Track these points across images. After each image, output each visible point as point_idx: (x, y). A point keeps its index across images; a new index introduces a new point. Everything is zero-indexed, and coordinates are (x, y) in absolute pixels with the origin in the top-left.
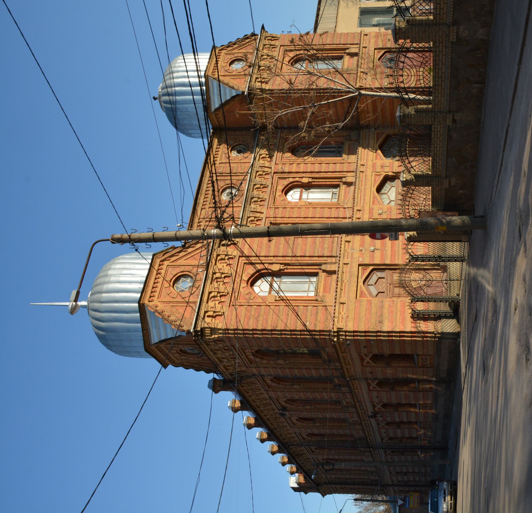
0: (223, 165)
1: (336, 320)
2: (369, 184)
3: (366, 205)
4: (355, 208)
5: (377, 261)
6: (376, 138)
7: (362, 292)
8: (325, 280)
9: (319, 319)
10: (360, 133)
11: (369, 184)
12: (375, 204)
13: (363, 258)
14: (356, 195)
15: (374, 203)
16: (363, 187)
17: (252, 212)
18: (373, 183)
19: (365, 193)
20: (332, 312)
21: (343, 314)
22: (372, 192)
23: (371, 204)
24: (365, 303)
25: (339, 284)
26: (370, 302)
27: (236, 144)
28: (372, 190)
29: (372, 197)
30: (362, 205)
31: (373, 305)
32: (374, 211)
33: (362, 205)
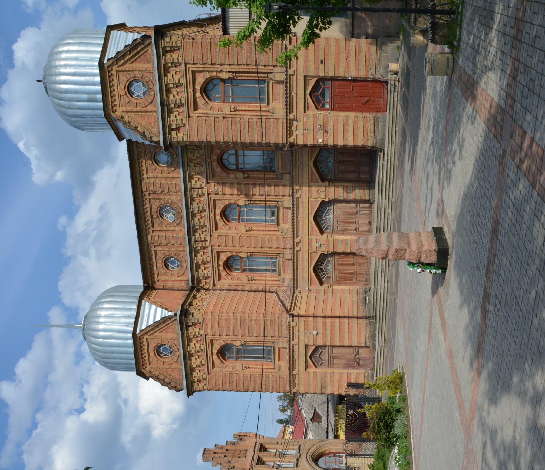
0: (152, 181)
3: (304, 237)
6: (310, 152)
8: (279, 351)
11: (306, 212)
13: (308, 340)
16: (300, 215)
20: (288, 380)
32: (313, 244)
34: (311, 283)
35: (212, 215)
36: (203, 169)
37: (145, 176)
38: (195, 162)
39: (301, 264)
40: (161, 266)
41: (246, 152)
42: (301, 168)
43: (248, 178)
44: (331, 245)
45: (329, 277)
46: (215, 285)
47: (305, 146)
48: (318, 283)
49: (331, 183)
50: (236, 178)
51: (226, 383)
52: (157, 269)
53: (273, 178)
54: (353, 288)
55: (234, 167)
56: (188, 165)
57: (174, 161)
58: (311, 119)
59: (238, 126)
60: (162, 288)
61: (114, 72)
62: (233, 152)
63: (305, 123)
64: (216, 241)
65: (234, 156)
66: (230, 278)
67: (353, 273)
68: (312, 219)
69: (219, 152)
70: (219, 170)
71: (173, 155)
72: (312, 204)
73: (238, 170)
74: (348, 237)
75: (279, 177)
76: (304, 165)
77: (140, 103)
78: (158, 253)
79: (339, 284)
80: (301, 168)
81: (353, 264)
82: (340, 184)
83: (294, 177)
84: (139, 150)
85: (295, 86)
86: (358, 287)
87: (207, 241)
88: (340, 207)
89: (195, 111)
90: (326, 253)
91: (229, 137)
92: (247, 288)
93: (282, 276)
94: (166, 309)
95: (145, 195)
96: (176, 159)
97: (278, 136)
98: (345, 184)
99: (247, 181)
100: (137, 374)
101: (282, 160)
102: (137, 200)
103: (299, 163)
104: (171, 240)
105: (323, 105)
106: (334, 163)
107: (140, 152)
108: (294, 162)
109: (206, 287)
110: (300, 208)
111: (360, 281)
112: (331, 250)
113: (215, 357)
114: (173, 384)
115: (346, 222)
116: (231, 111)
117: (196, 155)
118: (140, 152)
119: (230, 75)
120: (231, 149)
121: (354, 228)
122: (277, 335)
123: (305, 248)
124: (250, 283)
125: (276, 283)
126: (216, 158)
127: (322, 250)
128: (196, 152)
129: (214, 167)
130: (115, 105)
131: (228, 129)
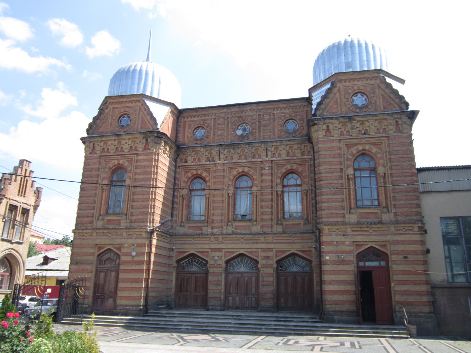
1: (81, 231)
2: (247, 246)
3: (224, 245)
4: (220, 237)
5: (123, 258)
7: (102, 248)
9: (84, 219)
10: (310, 233)
11: (247, 246)
12: (227, 254)
13: (126, 247)
14: (234, 236)
15: (226, 252)
16: (244, 241)
17: (220, 152)
18: (249, 250)
19: (238, 243)
21: (86, 235)
22: (239, 250)
23: (225, 250)
24: (92, 250)
25: (107, 231)
26: (93, 254)
27: (298, 121)
28: (241, 250)
29: (233, 250)
30: (224, 242)
31: (89, 257)
33: (224, 242)
34: (179, 252)
35: (243, 164)
36: (284, 157)
37: (276, 112)
38: (290, 151)
39: (197, 242)
40: (197, 123)
41: (299, 194)
42: (289, 241)
43: (277, 195)
44: (216, 270)
45: (184, 269)
46: (179, 166)
47: (320, 244)
48: (179, 258)
49: (275, 270)
50: (277, 185)
51: (91, 171)
52: (195, 121)
53: (278, 216)
54: (173, 291)
55: (285, 183)
56: (287, 145)
57: (290, 134)
58: (348, 248)
59: (336, 182)
60: (179, 124)
61: (373, 81)
62: (299, 182)
63: (343, 243)
64: (219, 168)
65: (295, 183)
66: (186, 180)
67: (187, 291)
68: (241, 252)
69: (300, 170)
70: (284, 170)
71: (294, 133)
72: (255, 252)
73: (284, 186)
74: (223, 287)
75: (279, 222)
76: (292, 244)
77: (348, 101)
78: (209, 122)
79: (177, 279)
80: (289, 241)
81: (196, 291)
82: (275, 279)
83: (280, 235)
84: (298, 107)
85: (379, 232)
86: (173, 296)
87: (220, 160)
88: (251, 278)
89: (346, 144)
90: (208, 265)
91: (324, 173)
92: (176, 194)
93: (187, 225)
94: (163, 122)
95: (260, 111)
96: (291, 136)
97: (329, 217)
98: (275, 283)
99: (275, 193)
100: (106, 97)
101: (295, 224)
102: (255, 105)
103: (294, 239)
104: (220, 132)
105: (361, 260)
106: (293, 273)
107: (296, 108)
108: (294, 235)
109: (178, 160)
110: (251, 241)
111: (180, 298)
112: (211, 270)
113: (116, 162)
114: (94, 126)
115: (237, 285)
116: (348, 175)
117: (296, 151)
118: (296, 108)
119: (382, 174)
120: (301, 181)
121: (231, 292)
122: (134, 218)
123: (213, 246)
124: (180, 197)
125: (180, 220)
126: (294, 168)
127: (211, 262)
128: (299, 151)
129: (286, 167)
130: (345, 82)
131: (332, 173)
